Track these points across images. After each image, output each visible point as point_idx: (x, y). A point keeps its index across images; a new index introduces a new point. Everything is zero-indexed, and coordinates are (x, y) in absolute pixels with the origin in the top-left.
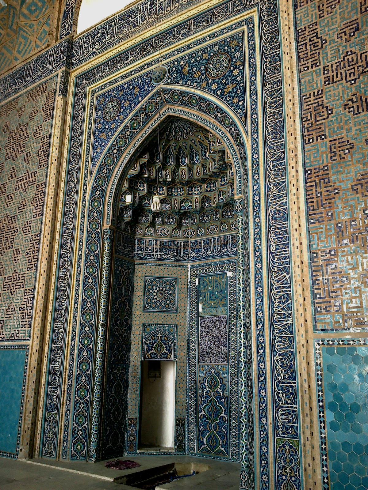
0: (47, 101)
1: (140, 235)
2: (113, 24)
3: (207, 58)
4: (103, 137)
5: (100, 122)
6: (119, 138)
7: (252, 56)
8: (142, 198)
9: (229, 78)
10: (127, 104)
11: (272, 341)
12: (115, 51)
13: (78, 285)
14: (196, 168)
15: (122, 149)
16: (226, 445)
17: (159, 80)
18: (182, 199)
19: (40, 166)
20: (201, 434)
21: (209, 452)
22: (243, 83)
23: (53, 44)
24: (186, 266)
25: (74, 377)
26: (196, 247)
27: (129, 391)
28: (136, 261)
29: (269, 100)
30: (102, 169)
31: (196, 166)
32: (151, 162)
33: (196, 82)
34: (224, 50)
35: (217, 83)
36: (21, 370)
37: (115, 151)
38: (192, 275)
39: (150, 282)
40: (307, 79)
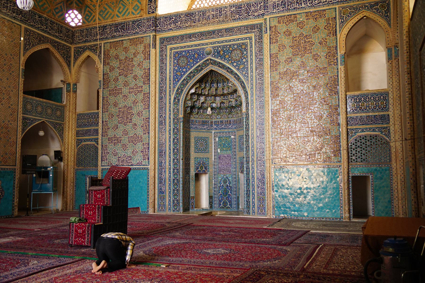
0: (145, 49)
1: (192, 118)
2: (182, 16)
4: (178, 74)
5: (176, 66)
7: (251, 55)
8: (195, 102)
10: (191, 61)
11: (257, 166)
12: (184, 32)
13: (170, 141)
16: (231, 205)
19: (144, 84)
20: (220, 201)
21: (223, 208)
23: (145, 16)
24: (212, 132)
25: (172, 180)
26: (217, 123)
27: (191, 186)
28: (191, 130)
29: (258, 77)
31: (219, 88)
36: (146, 178)
38: (214, 136)
39: (197, 139)
40: (273, 75)
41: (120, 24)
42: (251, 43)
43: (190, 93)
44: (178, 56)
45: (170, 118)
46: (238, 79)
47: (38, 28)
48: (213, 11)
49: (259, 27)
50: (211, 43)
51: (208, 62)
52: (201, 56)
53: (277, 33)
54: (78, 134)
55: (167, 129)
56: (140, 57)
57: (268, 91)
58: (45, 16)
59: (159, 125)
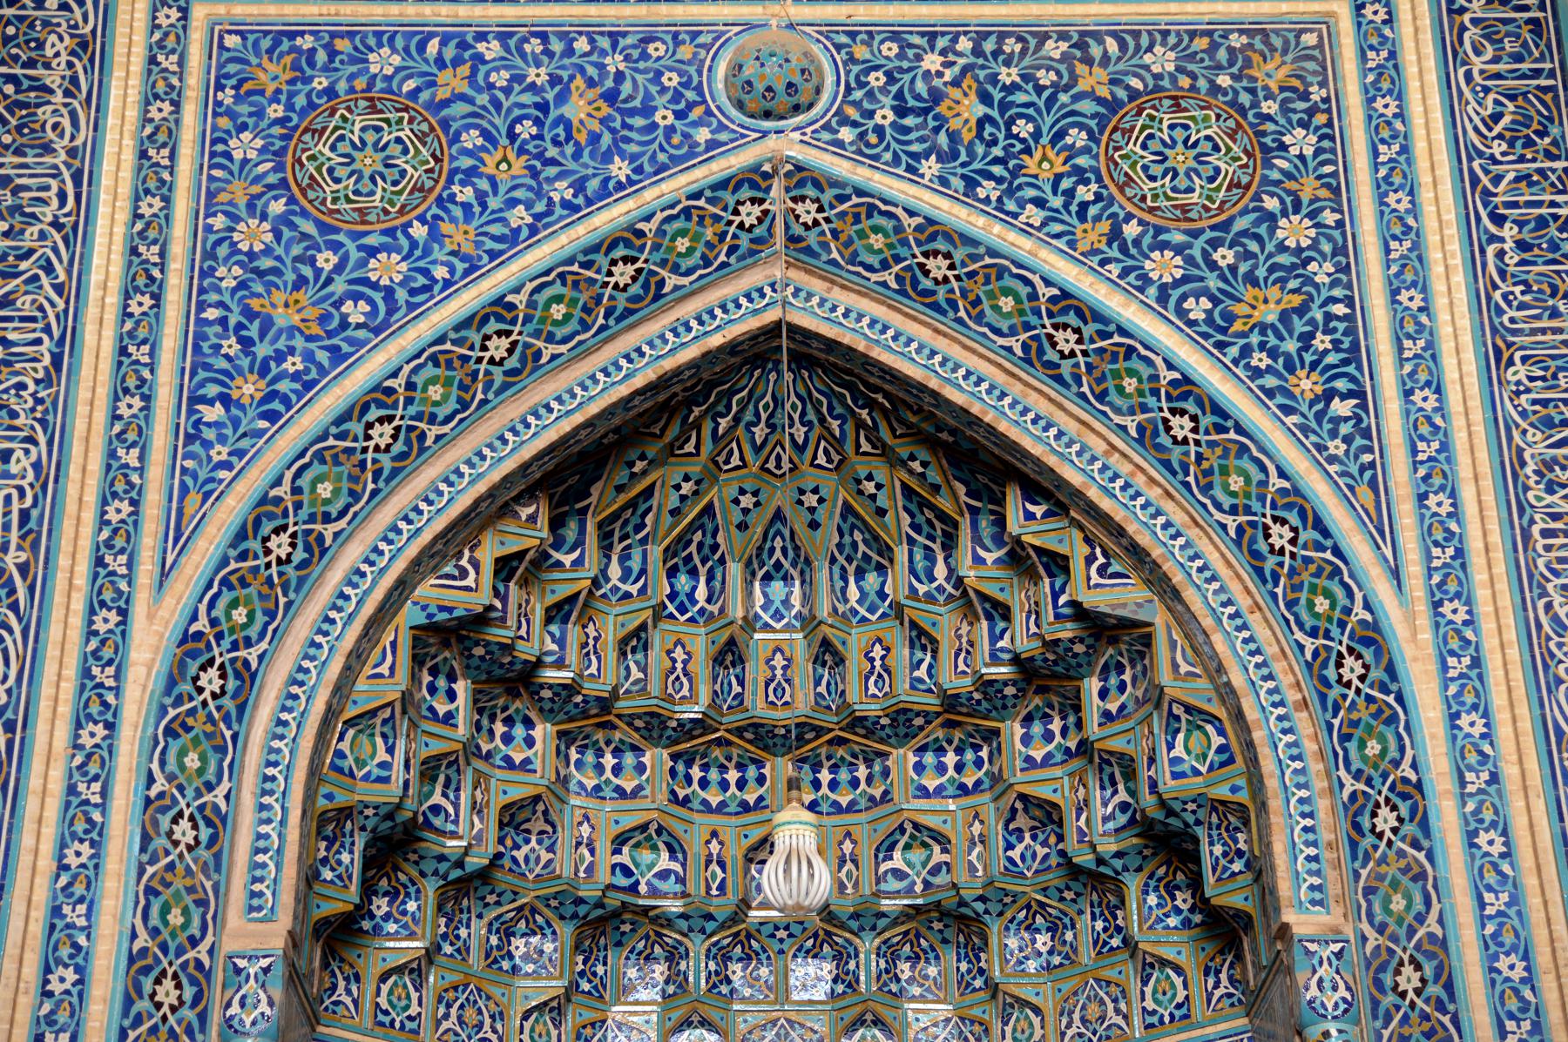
3: (1103, 92)
4: (283, 318)
6: (434, 359)
7: (1395, 176)
9: (1253, 246)
14: (764, 653)
15: (433, 432)
17: (774, 104)
18: (629, 821)
22: (1349, 301)
29: (1536, 445)
30: (267, 528)
33: (1040, 203)
34: (1215, 89)
35: (1179, 250)
37: (381, 435)
43: (410, 615)
51: (749, 214)
52: (664, 117)
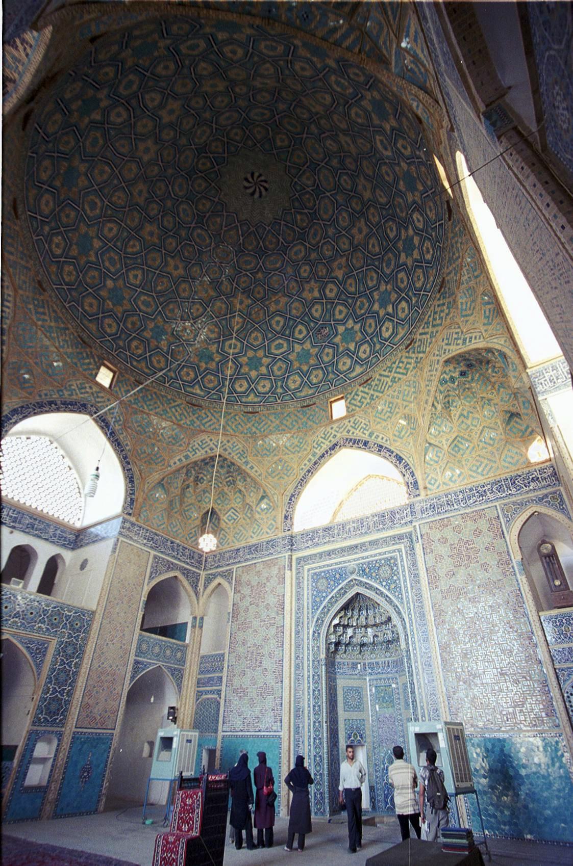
1: (338, 660)
7: (403, 571)
19: (278, 614)
25: (312, 757)
32: (345, 615)
39: (348, 690)
41: (253, 546)
42: (401, 556)
44: (316, 577)
45: (308, 660)
46: (390, 602)
47: (168, 555)
48: (353, 522)
49: (409, 536)
50: (354, 560)
53: (431, 541)
54: (199, 683)
55: (306, 677)
56: (274, 581)
57: (430, 616)
58: (178, 541)
59: (296, 670)
